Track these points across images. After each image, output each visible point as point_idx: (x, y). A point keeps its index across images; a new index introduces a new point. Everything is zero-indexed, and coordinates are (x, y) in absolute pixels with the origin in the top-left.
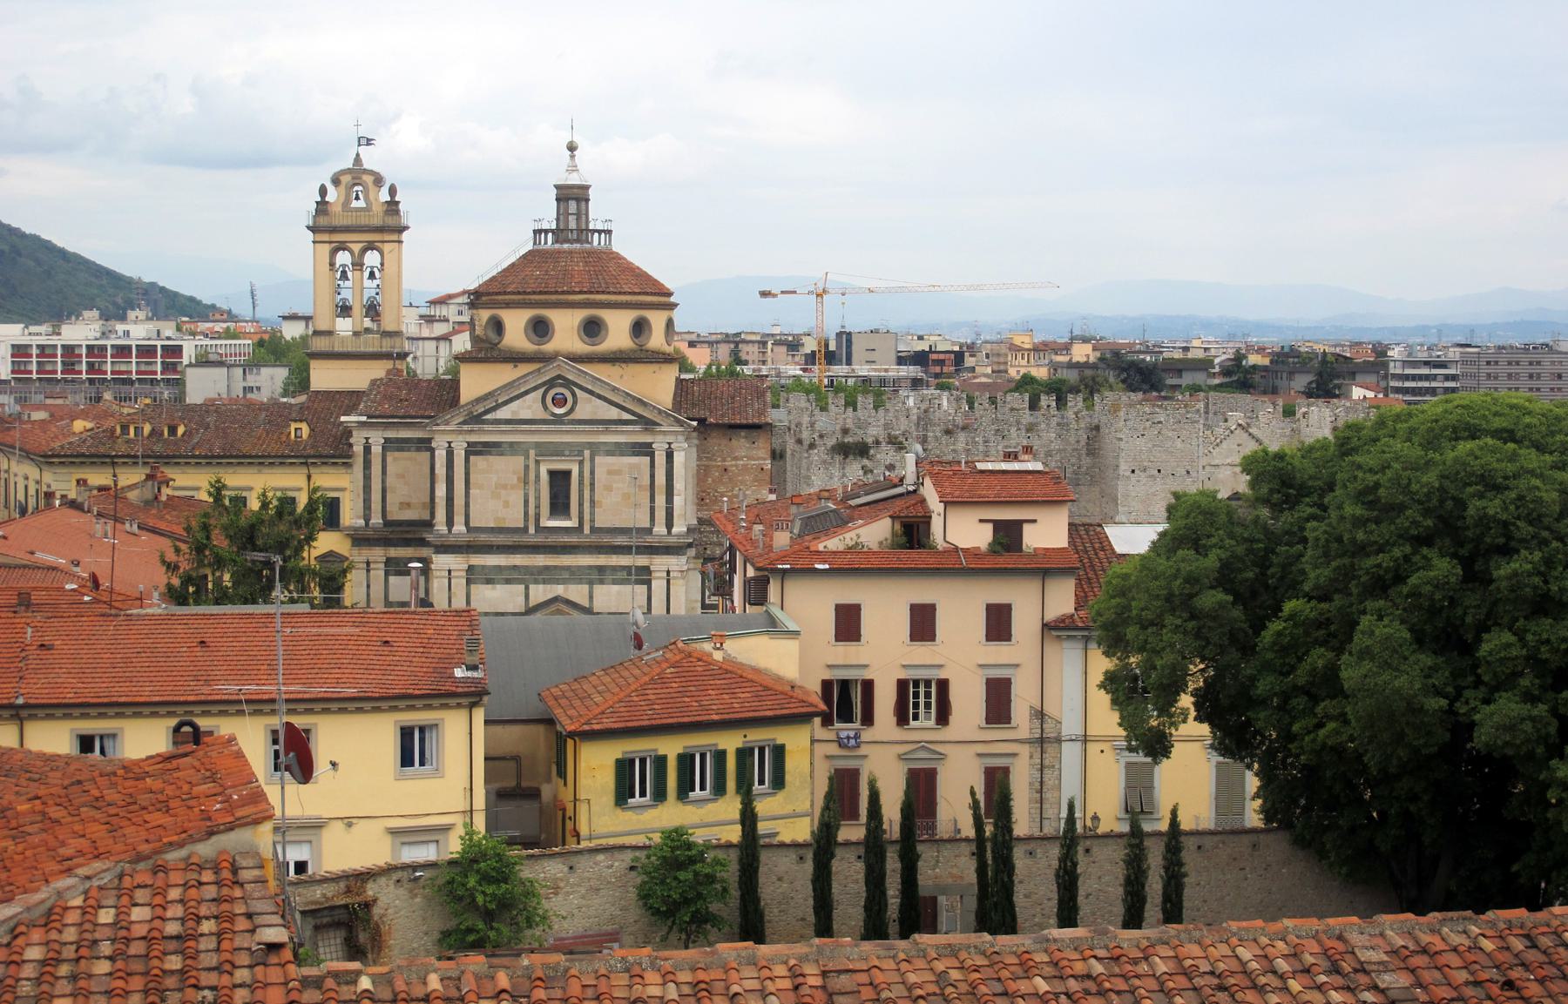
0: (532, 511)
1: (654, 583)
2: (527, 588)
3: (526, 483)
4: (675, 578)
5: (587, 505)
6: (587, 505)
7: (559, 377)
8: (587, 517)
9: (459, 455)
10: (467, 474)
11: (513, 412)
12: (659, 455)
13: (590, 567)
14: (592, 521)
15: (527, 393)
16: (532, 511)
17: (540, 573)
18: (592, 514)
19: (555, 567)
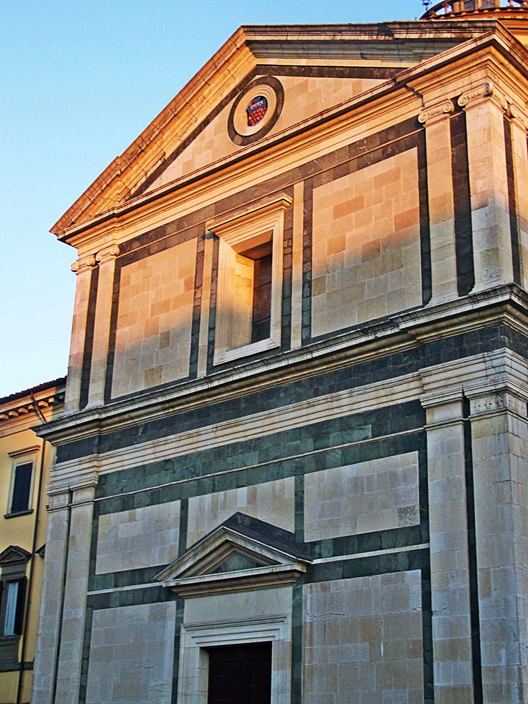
0: (203, 342)
1: (432, 439)
2: (184, 507)
3: (198, 287)
4: (481, 416)
5: (297, 295)
6: (297, 295)
7: (258, 69)
8: (296, 320)
9: (106, 270)
10: (115, 302)
11: (186, 165)
12: (435, 133)
13: (298, 433)
14: (306, 326)
15: (206, 122)
16: (203, 342)
17: (207, 467)
18: (307, 311)
19: (234, 446)
